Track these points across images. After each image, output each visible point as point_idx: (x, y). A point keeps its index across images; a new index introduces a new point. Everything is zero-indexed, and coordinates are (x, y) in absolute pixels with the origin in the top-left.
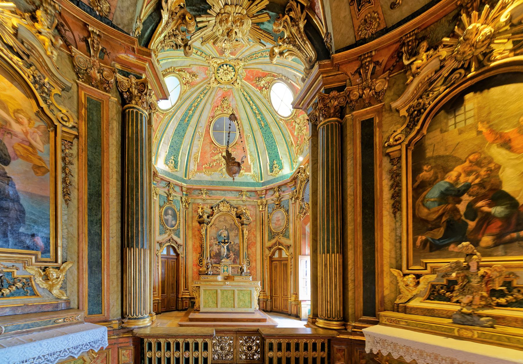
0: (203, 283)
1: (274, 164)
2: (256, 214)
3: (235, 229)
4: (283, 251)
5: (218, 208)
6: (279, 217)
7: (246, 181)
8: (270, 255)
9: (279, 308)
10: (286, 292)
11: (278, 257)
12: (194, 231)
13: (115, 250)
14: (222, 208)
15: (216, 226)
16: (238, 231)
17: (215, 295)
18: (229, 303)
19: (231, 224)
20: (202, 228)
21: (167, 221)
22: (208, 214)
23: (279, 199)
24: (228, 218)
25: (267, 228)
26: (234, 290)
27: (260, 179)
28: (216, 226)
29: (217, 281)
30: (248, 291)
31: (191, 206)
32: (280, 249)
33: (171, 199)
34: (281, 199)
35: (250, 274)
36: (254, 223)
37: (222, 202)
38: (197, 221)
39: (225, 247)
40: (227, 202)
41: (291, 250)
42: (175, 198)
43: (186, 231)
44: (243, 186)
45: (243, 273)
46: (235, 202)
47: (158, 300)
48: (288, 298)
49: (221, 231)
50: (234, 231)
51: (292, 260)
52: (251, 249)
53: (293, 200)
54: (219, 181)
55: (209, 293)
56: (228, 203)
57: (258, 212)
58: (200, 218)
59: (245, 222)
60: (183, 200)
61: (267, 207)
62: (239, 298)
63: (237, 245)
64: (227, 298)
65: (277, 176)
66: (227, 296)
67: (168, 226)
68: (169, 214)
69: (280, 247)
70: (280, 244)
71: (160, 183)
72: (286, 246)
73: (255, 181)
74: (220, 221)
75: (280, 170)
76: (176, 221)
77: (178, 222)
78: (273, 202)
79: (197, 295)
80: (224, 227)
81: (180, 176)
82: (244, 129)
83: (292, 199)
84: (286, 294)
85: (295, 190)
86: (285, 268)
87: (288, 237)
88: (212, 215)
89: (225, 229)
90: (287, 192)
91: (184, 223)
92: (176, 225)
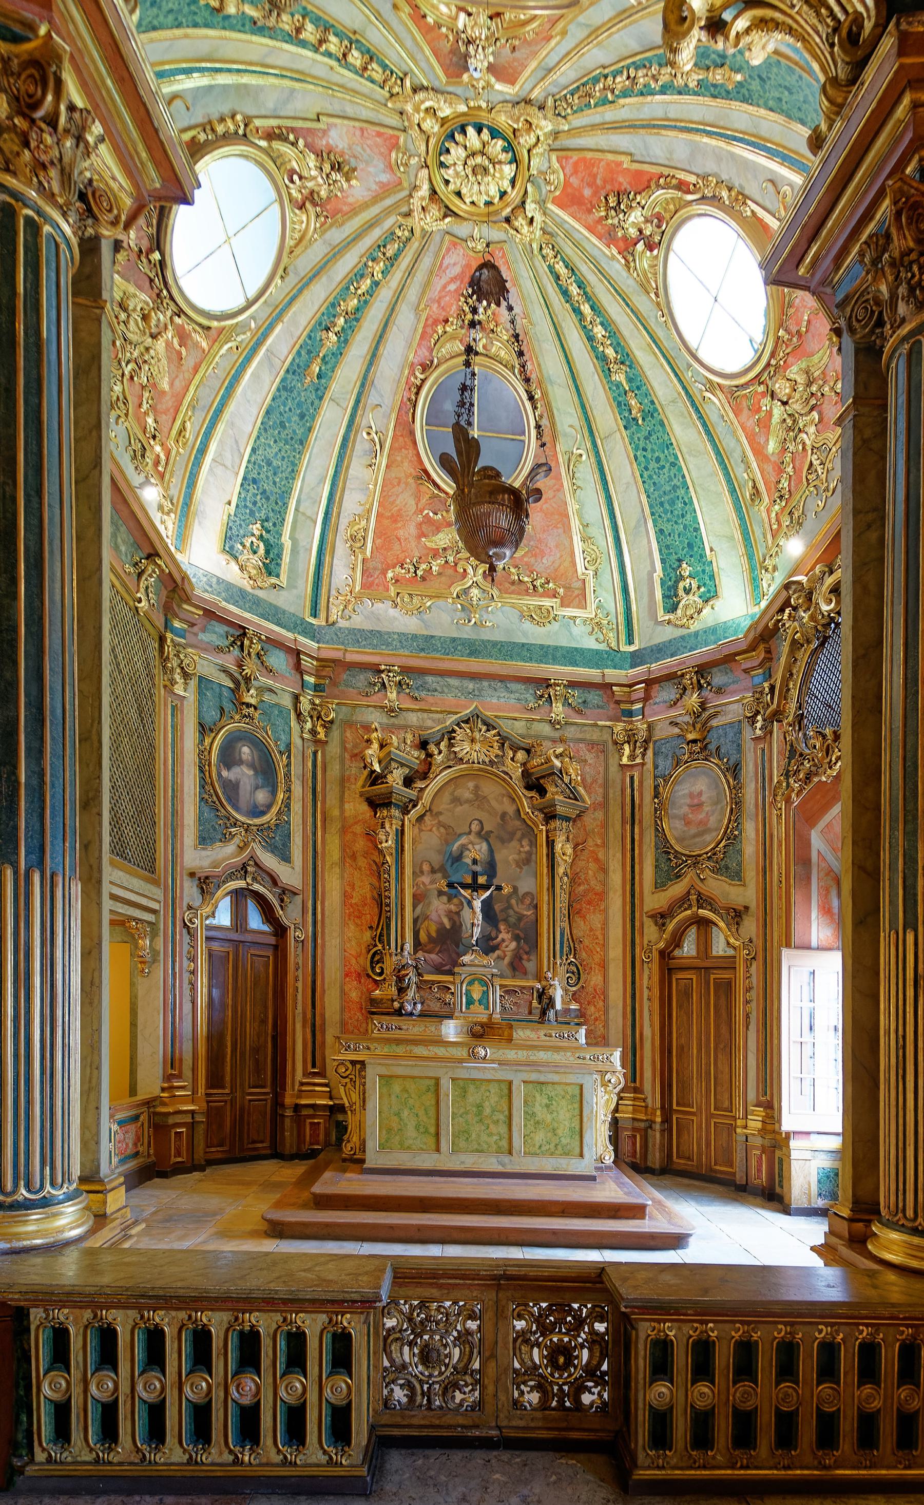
2: (606, 780)
3: (519, 834)
14: (467, 747)
16: (533, 843)
19: (504, 815)
20: (383, 826)
21: (232, 788)
24: (490, 789)
28: (441, 818)
35: (582, 1017)
43: (315, 834)
45: (551, 1014)
49: (463, 840)
50: (514, 843)
52: (584, 917)
53: (759, 725)
57: (613, 769)
58: (373, 784)
61: (650, 753)
67: (237, 809)
76: (274, 793)
78: (676, 730)
80: (475, 827)
83: (752, 720)
85: (766, 685)
88: (424, 776)
89: (479, 834)
90: (734, 693)
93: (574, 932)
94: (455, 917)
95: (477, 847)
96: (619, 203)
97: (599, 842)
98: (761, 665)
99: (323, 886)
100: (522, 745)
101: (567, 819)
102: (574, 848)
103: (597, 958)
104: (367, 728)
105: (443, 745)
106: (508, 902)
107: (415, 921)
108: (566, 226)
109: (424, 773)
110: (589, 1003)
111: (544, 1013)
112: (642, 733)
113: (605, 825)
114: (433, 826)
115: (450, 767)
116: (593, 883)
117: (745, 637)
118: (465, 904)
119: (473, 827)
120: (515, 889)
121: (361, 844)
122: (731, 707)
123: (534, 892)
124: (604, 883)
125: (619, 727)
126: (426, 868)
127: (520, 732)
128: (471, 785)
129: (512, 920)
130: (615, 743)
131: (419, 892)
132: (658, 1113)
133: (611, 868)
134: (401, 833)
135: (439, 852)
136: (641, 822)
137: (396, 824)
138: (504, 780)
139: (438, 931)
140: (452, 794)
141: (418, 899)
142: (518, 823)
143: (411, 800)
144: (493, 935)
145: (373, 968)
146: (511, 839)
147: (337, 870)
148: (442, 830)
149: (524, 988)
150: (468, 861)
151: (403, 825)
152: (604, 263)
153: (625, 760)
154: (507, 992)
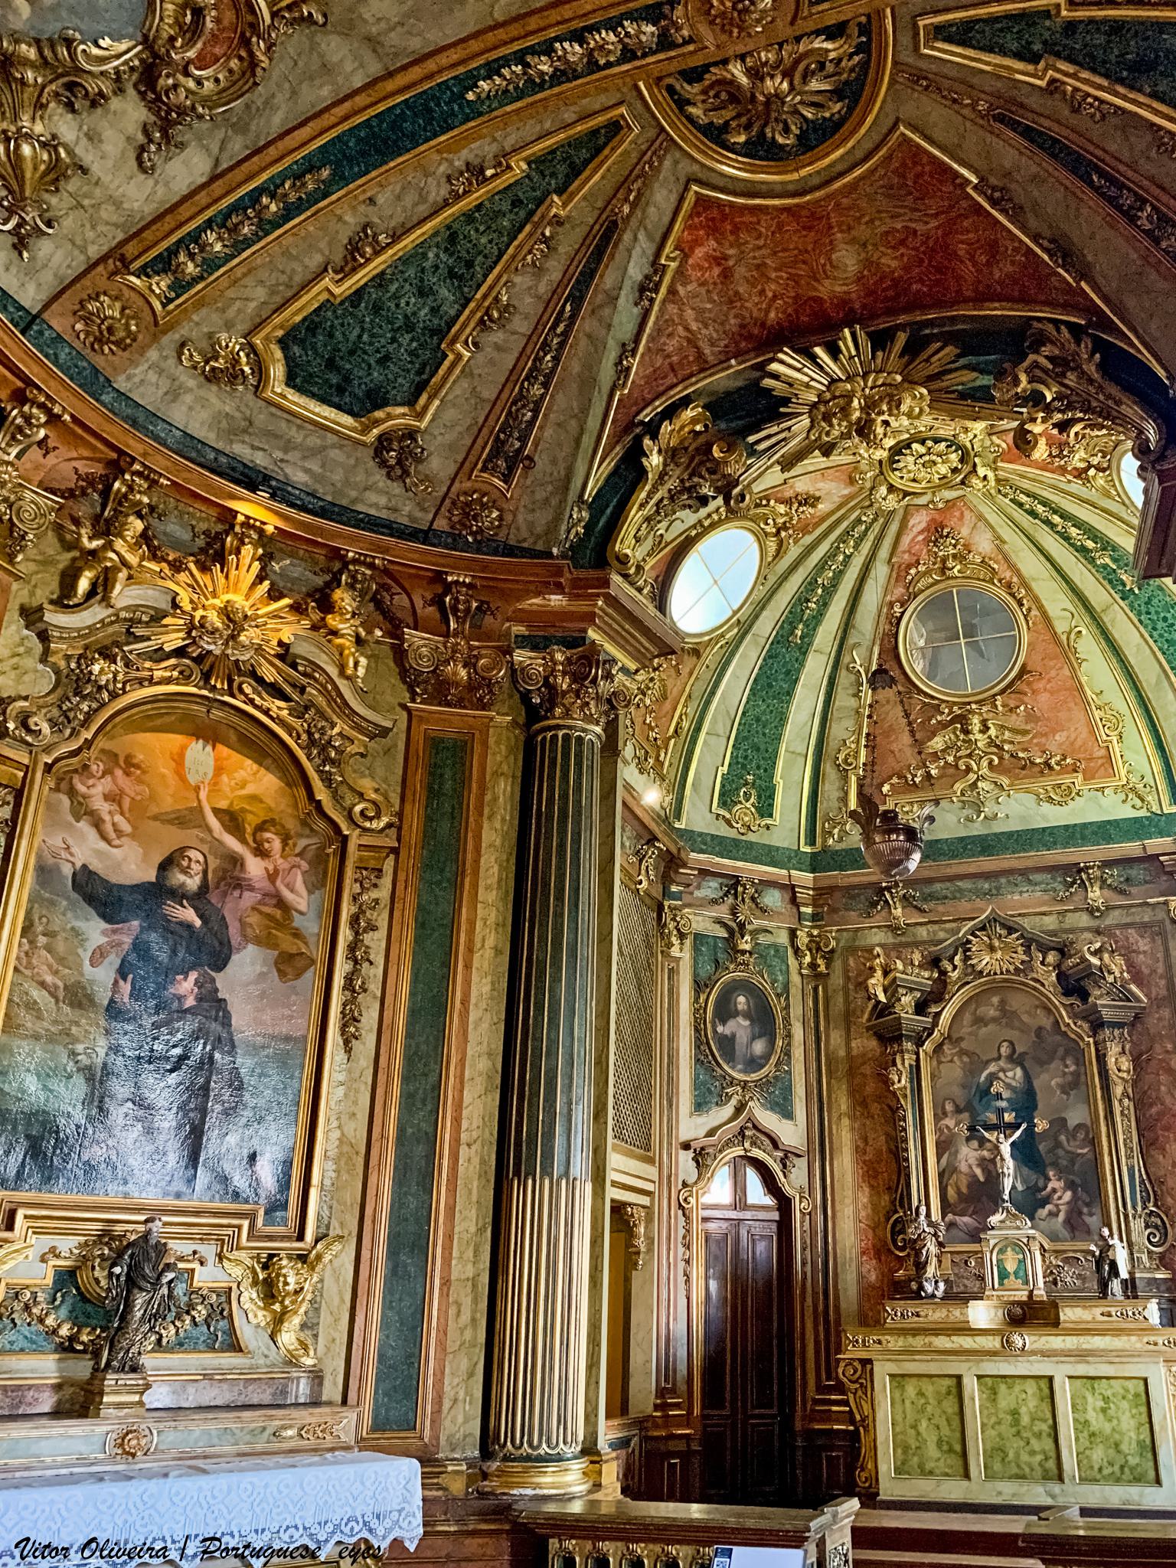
0: (895, 1343)
12: (858, 1080)
13: (475, 1191)
15: (964, 1045)
17: (950, 1406)
20: (894, 1064)
21: (727, 1044)
24: (1018, 1002)
28: (964, 1045)
29: (965, 1329)
31: (838, 964)
33: (747, 947)
37: (983, 928)
38: (868, 1029)
40: (1003, 926)
42: (763, 939)
46: (1050, 922)
49: (992, 1068)
54: (962, 839)
55: (921, 1394)
56: (1011, 930)
59: (1106, 1014)
60: (803, 939)
66: (1015, 1413)
68: (736, 1014)
71: (698, 887)
73: (1143, 813)
74: (979, 1021)
77: (779, 1043)
80: (1005, 1050)
81: (785, 845)
89: (1010, 1058)
91: (812, 1046)
92: (773, 1060)
99: (831, 1142)
114: (953, 1055)
119: (1003, 1050)
121: (871, 1088)
128: (995, 1000)
134: (916, 1070)
135: (964, 1086)
137: (909, 1058)
138: (1035, 989)
140: (974, 1013)
142: (1059, 1038)
143: (925, 1029)
147: (846, 1122)
148: (966, 1059)
151: (918, 1060)
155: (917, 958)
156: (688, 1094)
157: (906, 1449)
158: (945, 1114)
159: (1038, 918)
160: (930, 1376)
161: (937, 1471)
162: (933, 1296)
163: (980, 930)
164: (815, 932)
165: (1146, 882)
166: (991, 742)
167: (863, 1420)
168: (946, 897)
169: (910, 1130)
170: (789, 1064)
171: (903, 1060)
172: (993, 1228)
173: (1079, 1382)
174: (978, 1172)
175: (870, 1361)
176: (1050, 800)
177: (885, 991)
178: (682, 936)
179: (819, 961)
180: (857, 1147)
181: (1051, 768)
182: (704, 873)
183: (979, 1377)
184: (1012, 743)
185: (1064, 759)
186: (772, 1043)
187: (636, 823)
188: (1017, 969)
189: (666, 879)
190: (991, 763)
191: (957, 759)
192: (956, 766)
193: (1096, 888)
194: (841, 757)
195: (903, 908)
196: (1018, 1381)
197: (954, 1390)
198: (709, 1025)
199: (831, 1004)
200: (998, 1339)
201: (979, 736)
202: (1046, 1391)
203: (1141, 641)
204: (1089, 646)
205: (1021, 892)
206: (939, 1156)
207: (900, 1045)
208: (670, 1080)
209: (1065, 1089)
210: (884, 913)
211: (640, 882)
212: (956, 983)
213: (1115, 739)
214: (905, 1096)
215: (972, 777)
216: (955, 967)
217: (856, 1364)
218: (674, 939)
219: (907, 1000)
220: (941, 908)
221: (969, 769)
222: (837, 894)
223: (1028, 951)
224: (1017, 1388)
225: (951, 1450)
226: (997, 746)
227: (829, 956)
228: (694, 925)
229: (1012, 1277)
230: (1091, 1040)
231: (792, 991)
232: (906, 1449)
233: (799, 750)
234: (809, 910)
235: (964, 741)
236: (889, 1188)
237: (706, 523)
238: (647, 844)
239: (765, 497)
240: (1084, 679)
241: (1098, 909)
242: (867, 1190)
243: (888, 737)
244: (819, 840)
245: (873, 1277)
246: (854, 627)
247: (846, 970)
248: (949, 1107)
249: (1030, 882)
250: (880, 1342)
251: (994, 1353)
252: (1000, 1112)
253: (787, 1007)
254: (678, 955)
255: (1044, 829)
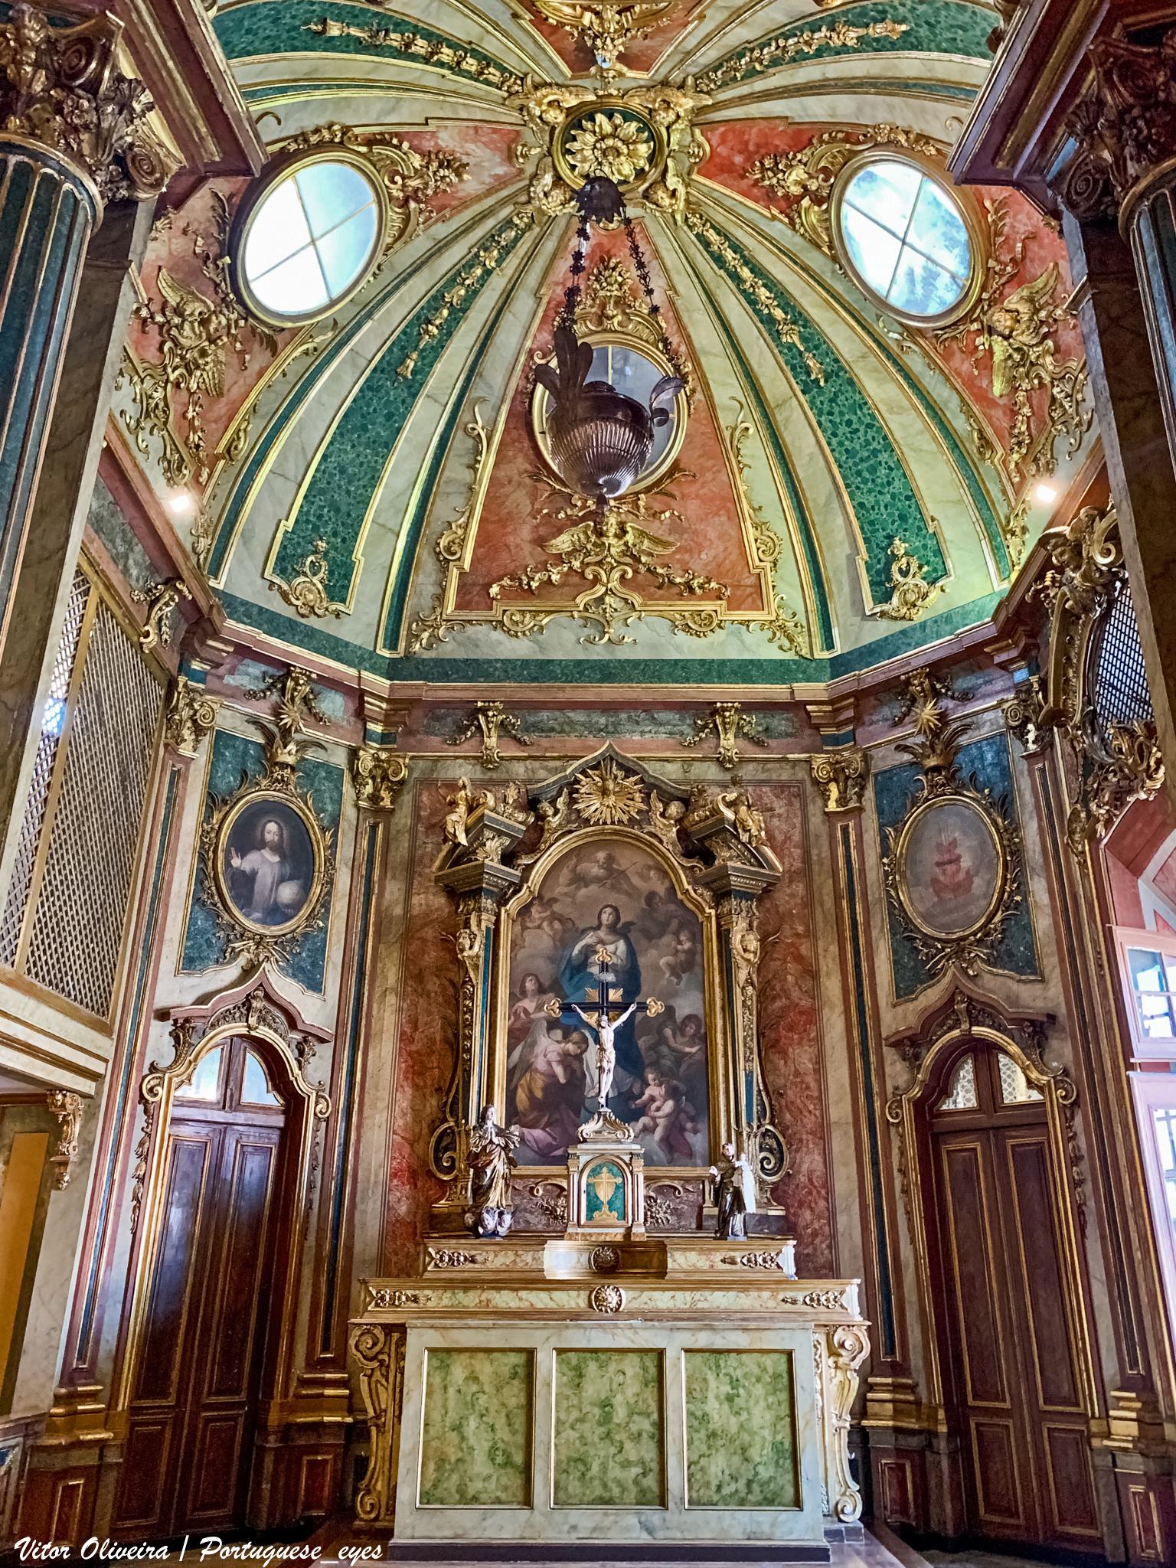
0: (436, 1300)
1: (895, 558)
2: (805, 833)
3: (675, 923)
4: (1003, 1059)
5: (572, 801)
6: (954, 844)
7: (733, 653)
8: (916, 1092)
9: (1030, 1517)
10: (1064, 1372)
11: (973, 1103)
16: (697, 936)
17: (514, 1395)
18: (626, 1464)
19: (651, 897)
21: (244, 884)
22: (507, 841)
23: (943, 736)
24: (629, 861)
25: (880, 920)
26: (660, 1353)
27: (818, 642)
28: (556, 908)
29: (537, 1281)
30: (768, 1361)
31: (407, 799)
32: (985, 1054)
33: (290, 760)
34: (957, 734)
35: (786, 1228)
36: (800, 888)
37: (596, 767)
38: (438, 880)
39: (608, 1036)
40: (621, 766)
41: (1062, 1051)
42: (311, 754)
43: (363, 945)
44: (721, 678)
45: (737, 1222)
47: (102, 1444)
48: (1084, 1418)
49: (589, 939)
50: (667, 939)
51: (1078, 1121)
52: (784, 1054)
54: (579, 663)
55: (473, 1378)
56: (629, 772)
57: (816, 820)
60: (366, 761)
61: (869, 793)
62: (698, 1419)
63: (690, 1030)
64: (606, 1419)
65: (919, 616)
66: (606, 1405)
68: (262, 845)
69: (980, 1030)
70: (980, 1011)
72: (1018, 1021)
73: (790, 656)
74: (579, 880)
75: (933, 583)
77: (316, 890)
78: (907, 757)
79: (385, 1398)
80: (607, 917)
81: (358, 643)
82: (717, 400)
83: (1021, 732)
84: (1066, 1388)
86: (1032, 1186)
87: (1029, 966)
89: (613, 928)
90: (985, 696)
92: (305, 911)
93: (770, 1078)
94: (573, 1063)
95: (611, 948)
96: (777, 164)
97: (800, 929)
98: (1022, 656)
100: (678, 794)
101: (747, 896)
102: (762, 941)
103: (810, 1122)
104: (453, 786)
105: (561, 803)
106: (660, 1031)
107: (511, 1073)
108: (715, 195)
109: (531, 842)
110: (801, 1205)
111: (724, 1221)
112: (854, 765)
113: (809, 903)
114: (543, 919)
115: (570, 832)
116: (795, 994)
117: (994, 619)
118: (591, 1041)
119: (604, 917)
120: (670, 1011)
121: (432, 956)
122: (987, 716)
123: (701, 1015)
124: (814, 993)
125: (819, 760)
126: (530, 985)
127: (674, 777)
128: (601, 855)
129: (667, 1063)
130: (816, 782)
131: (518, 1025)
132: (941, 1414)
133: (824, 969)
135: (551, 959)
136: (865, 895)
137: (487, 920)
138: (651, 845)
139: (545, 1089)
140: (574, 870)
141: (516, 1036)
142: (672, 907)
143: (511, 884)
144: (636, 1090)
145: (438, 1161)
146: (661, 935)
147: (391, 1000)
148: (557, 925)
149: (687, 1180)
150: (595, 970)
151: (497, 923)
152: (763, 225)
153: (832, 806)
154: (660, 1190)
155: (512, 794)
156: (176, 944)
157: (441, 1462)
158: (524, 994)
159: (658, 765)
160: (489, 1351)
161: (484, 1497)
162: (495, 1233)
163: (592, 768)
164: (384, 756)
165: (788, 735)
166: (627, 551)
167: (378, 1417)
168: (552, 730)
169: (478, 1011)
170: (325, 919)
171: (480, 921)
172: (585, 1141)
173: (698, 1357)
174: (559, 1071)
175: (402, 1329)
176: (687, 628)
177: (467, 832)
178: (199, 730)
179: (384, 794)
180: (403, 1033)
181: (691, 590)
182: (243, 651)
183: (560, 1351)
184: (651, 555)
185: (709, 582)
186: (306, 889)
187: (150, 543)
188: (631, 820)
189: (187, 649)
190: (623, 577)
191: (583, 564)
192: (582, 575)
193: (731, 736)
194: (443, 542)
195: (499, 737)
196: (616, 1356)
197: (521, 1371)
198: (221, 855)
199: (393, 846)
200: (584, 1294)
201: (613, 541)
202: (653, 1371)
203: (817, 450)
204: (755, 449)
205: (642, 733)
206: (510, 1050)
207: (477, 901)
208: (152, 922)
209: (676, 970)
210: (474, 742)
211: (147, 635)
212: (556, 830)
213: (769, 565)
214: (476, 967)
215: (600, 590)
216: (556, 812)
217: (377, 1332)
218: (187, 734)
219: (494, 846)
220: (545, 742)
221: (596, 580)
222: (417, 713)
223: (646, 799)
224: (613, 1367)
225: (508, 1463)
226: (633, 556)
227: (398, 789)
228: (218, 720)
229: (605, 1208)
230: (713, 912)
231: (343, 825)
232: (441, 1462)
233: (391, 524)
234: (377, 728)
235: (595, 544)
236: (439, 1090)
237: (314, 139)
238: (165, 583)
239: (397, 135)
240: (742, 488)
241: (731, 761)
242: (409, 1091)
243: (505, 526)
244: (402, 644)
245: (403, 1209)
246: (480, 375)
247: (417, 808)
248: (530, 985)
249: (654, 721)
250: (416, 1299)
251: (575, 1316)
252: (605, 987)
253: (334, 846)
254: (189, 754)
255: (676, 661)
